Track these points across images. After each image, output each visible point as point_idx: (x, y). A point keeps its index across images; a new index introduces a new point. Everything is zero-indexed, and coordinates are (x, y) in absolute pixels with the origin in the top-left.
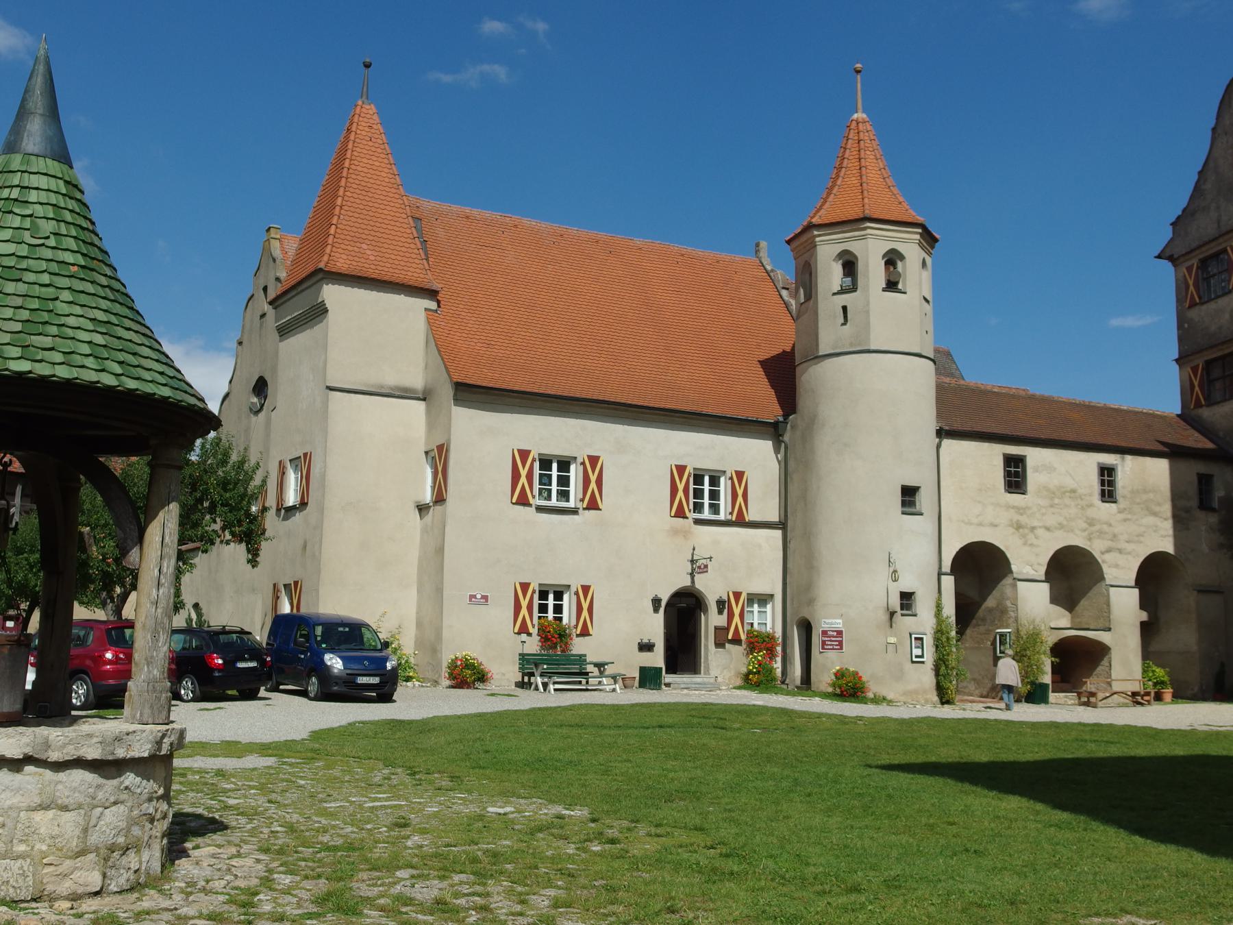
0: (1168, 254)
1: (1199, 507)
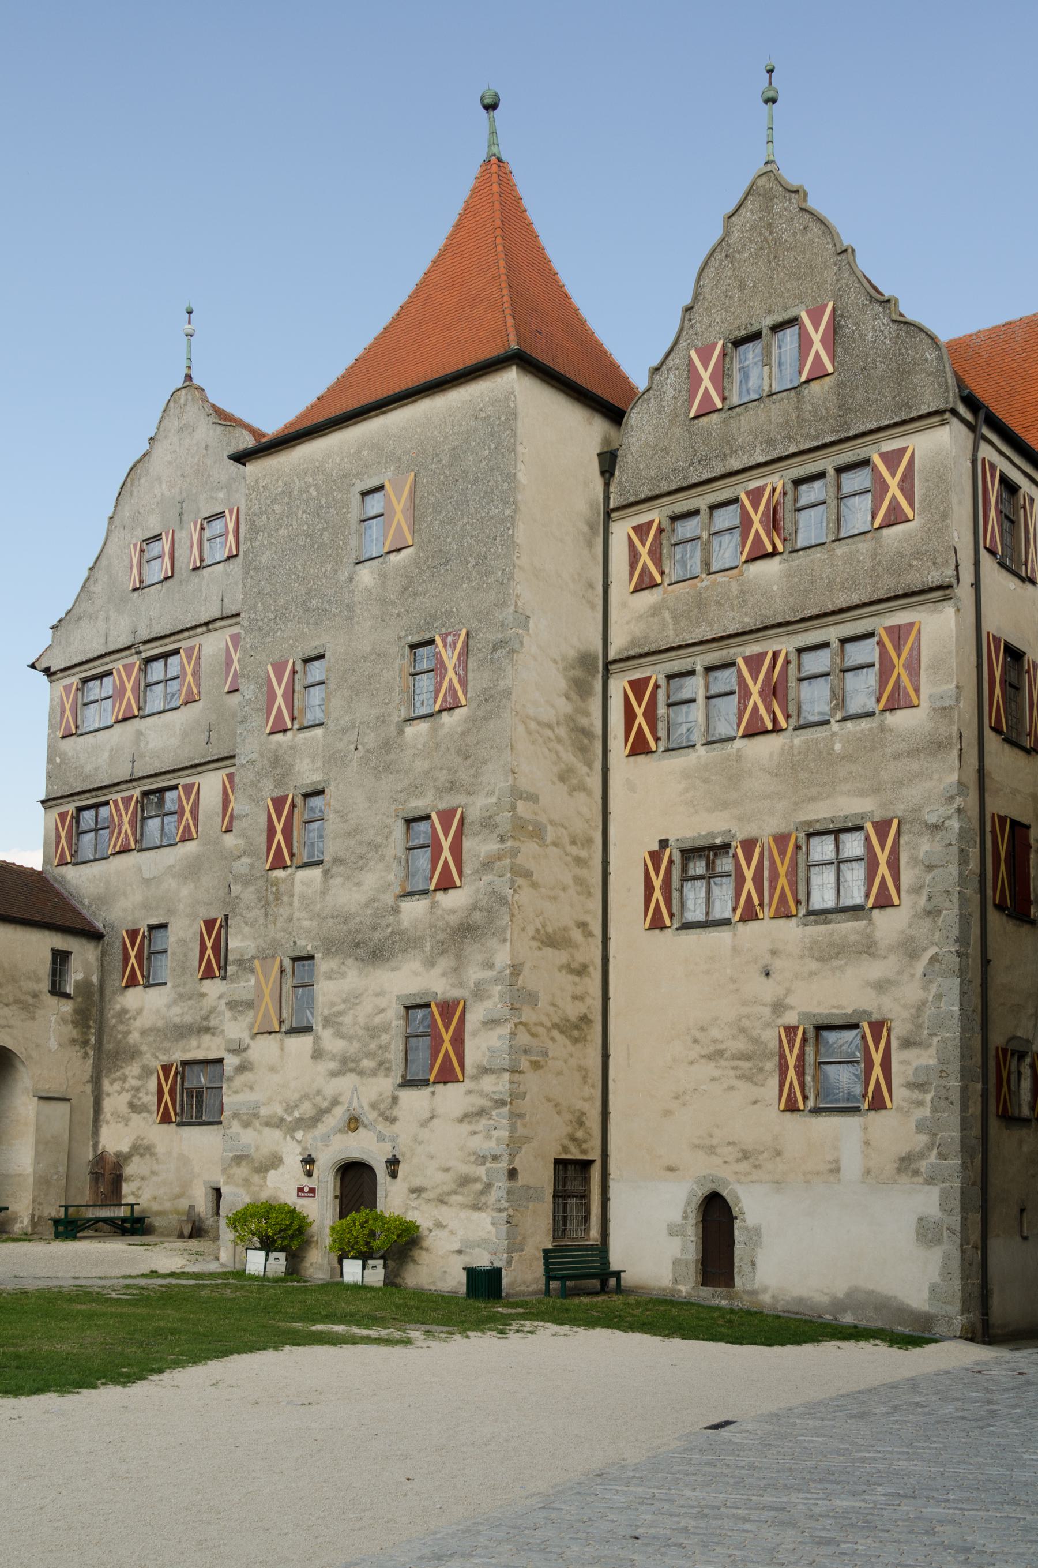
1: (49, 992)
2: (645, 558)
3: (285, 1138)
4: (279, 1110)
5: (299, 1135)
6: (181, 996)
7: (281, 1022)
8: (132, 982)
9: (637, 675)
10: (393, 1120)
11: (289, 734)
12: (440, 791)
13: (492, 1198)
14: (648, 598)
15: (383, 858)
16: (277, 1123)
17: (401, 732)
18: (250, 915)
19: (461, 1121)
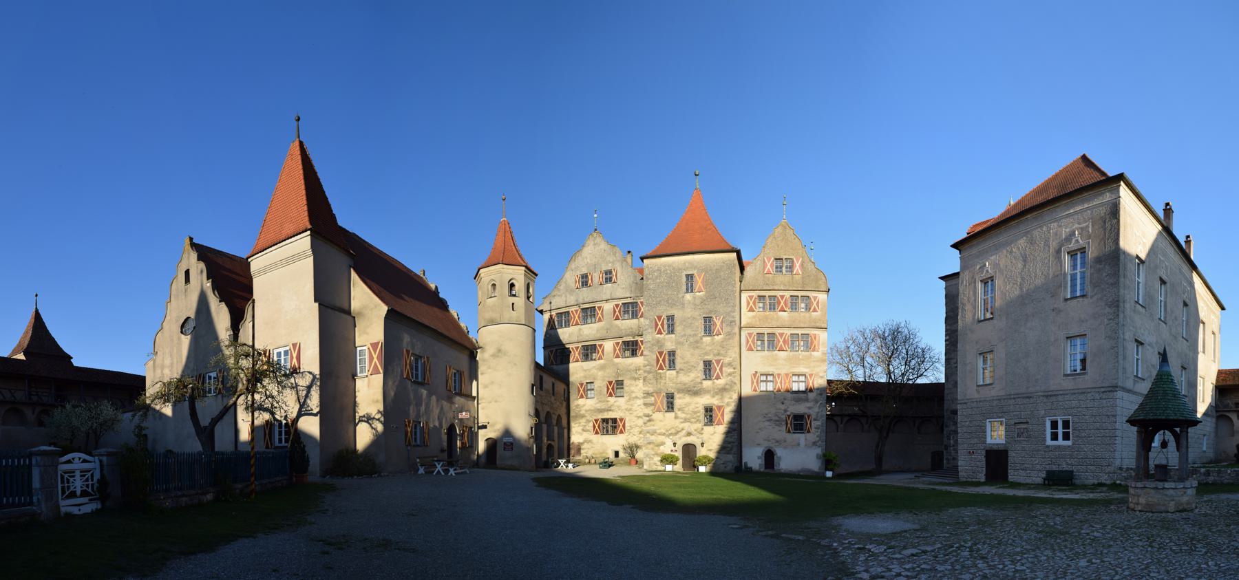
2: (751, 304)
5: (671, 437)
6: (600, 401)
8: (582, 397)
9: (749, 332)
10: (702, 434)
12: (715, 355)
14: (751, 314)
15: (696, 370)
16: (664, 434)
17: (701, 339)
18: (651, 382)
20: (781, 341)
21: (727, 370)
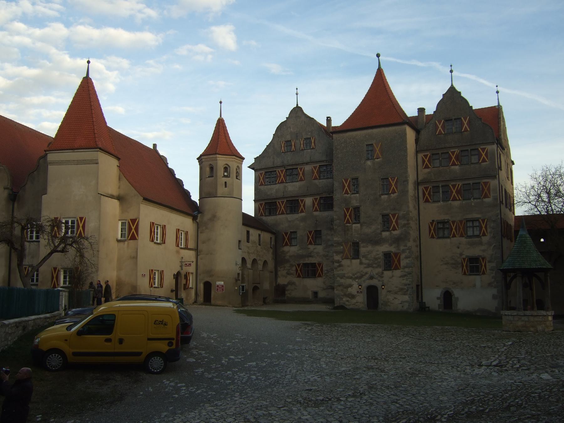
0: (252, 167)
3: (353, 281)
4: (351, 275)
5: (357, 280)
7: (351, 256)
8: (286, 245)
10: (383, 277)
11: (349, 195)
13: (409, 292)
14: (427, 170)
16: (351, 278)
17: (380, 196)
19: (400, 277)
20: (454, 191)
21: (402, 222)
